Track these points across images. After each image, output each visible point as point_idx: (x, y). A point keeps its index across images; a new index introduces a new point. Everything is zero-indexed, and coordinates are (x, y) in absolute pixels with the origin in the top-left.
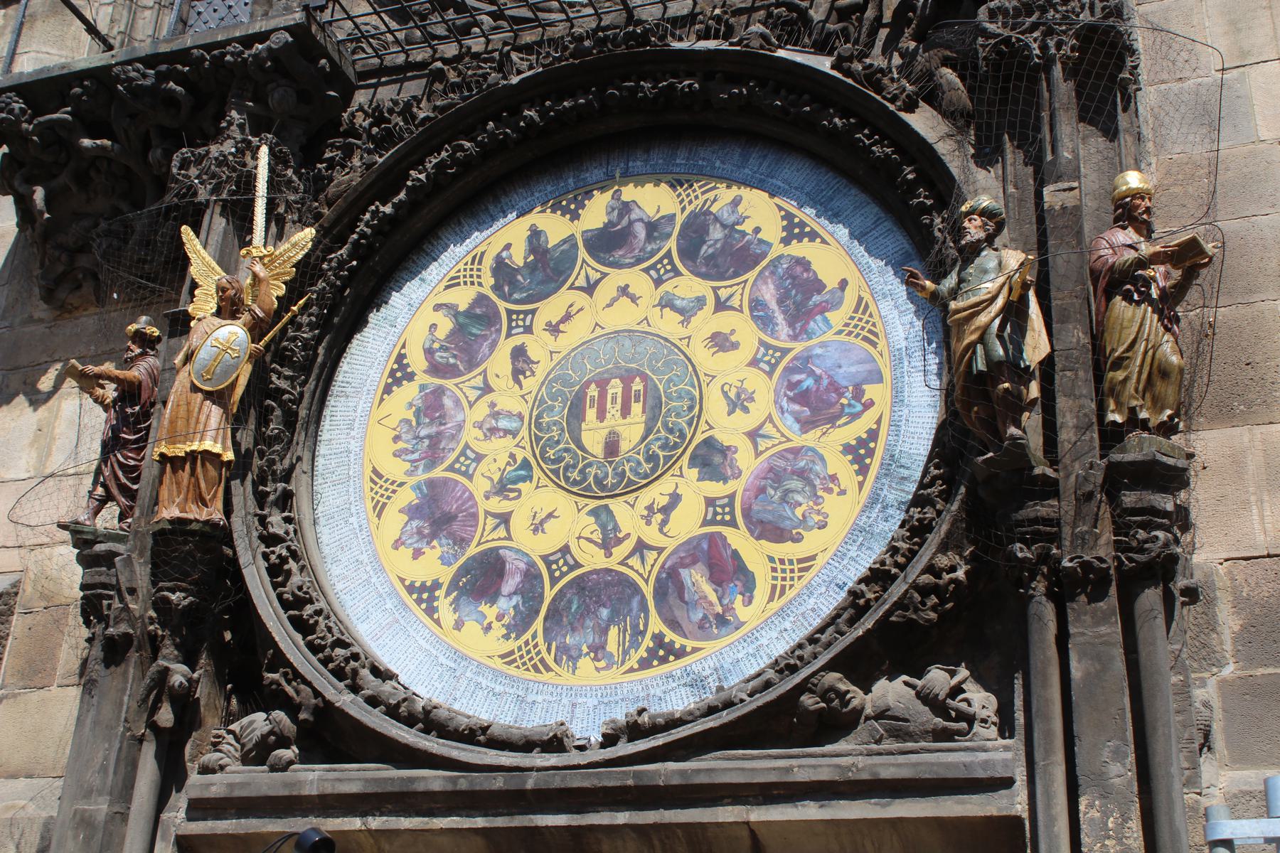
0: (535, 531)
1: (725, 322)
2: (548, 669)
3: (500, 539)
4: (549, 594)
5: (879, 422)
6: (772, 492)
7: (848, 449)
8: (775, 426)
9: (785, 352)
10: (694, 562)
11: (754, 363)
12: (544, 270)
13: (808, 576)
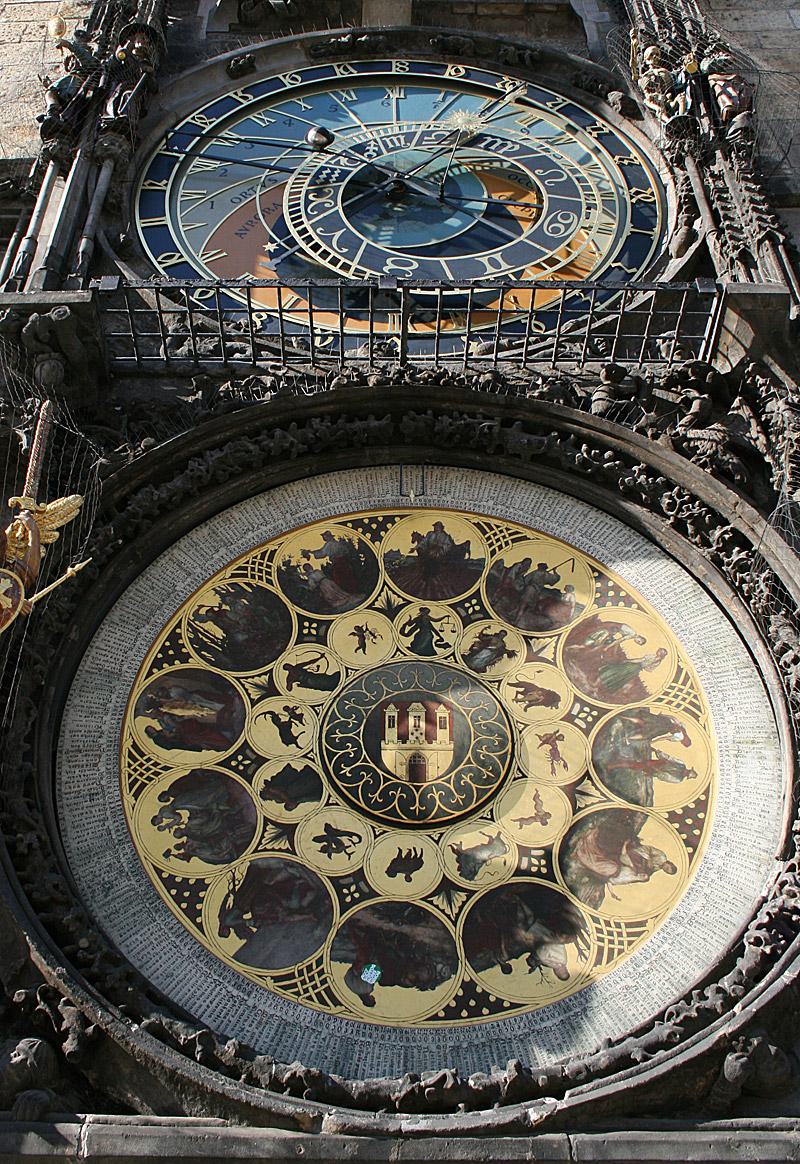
0: (358, 628)
1: (424, 881)
2: (233, 576)
3: (376, 600)
4: (294, 610)
5: (200, 926)
6: (221, 808)
7: (201, 885)
8: (280, 850)
9: (344, 908)
10: (220, 714)
11: (359, 875)
12: (629, 762)
13: (126, 782)
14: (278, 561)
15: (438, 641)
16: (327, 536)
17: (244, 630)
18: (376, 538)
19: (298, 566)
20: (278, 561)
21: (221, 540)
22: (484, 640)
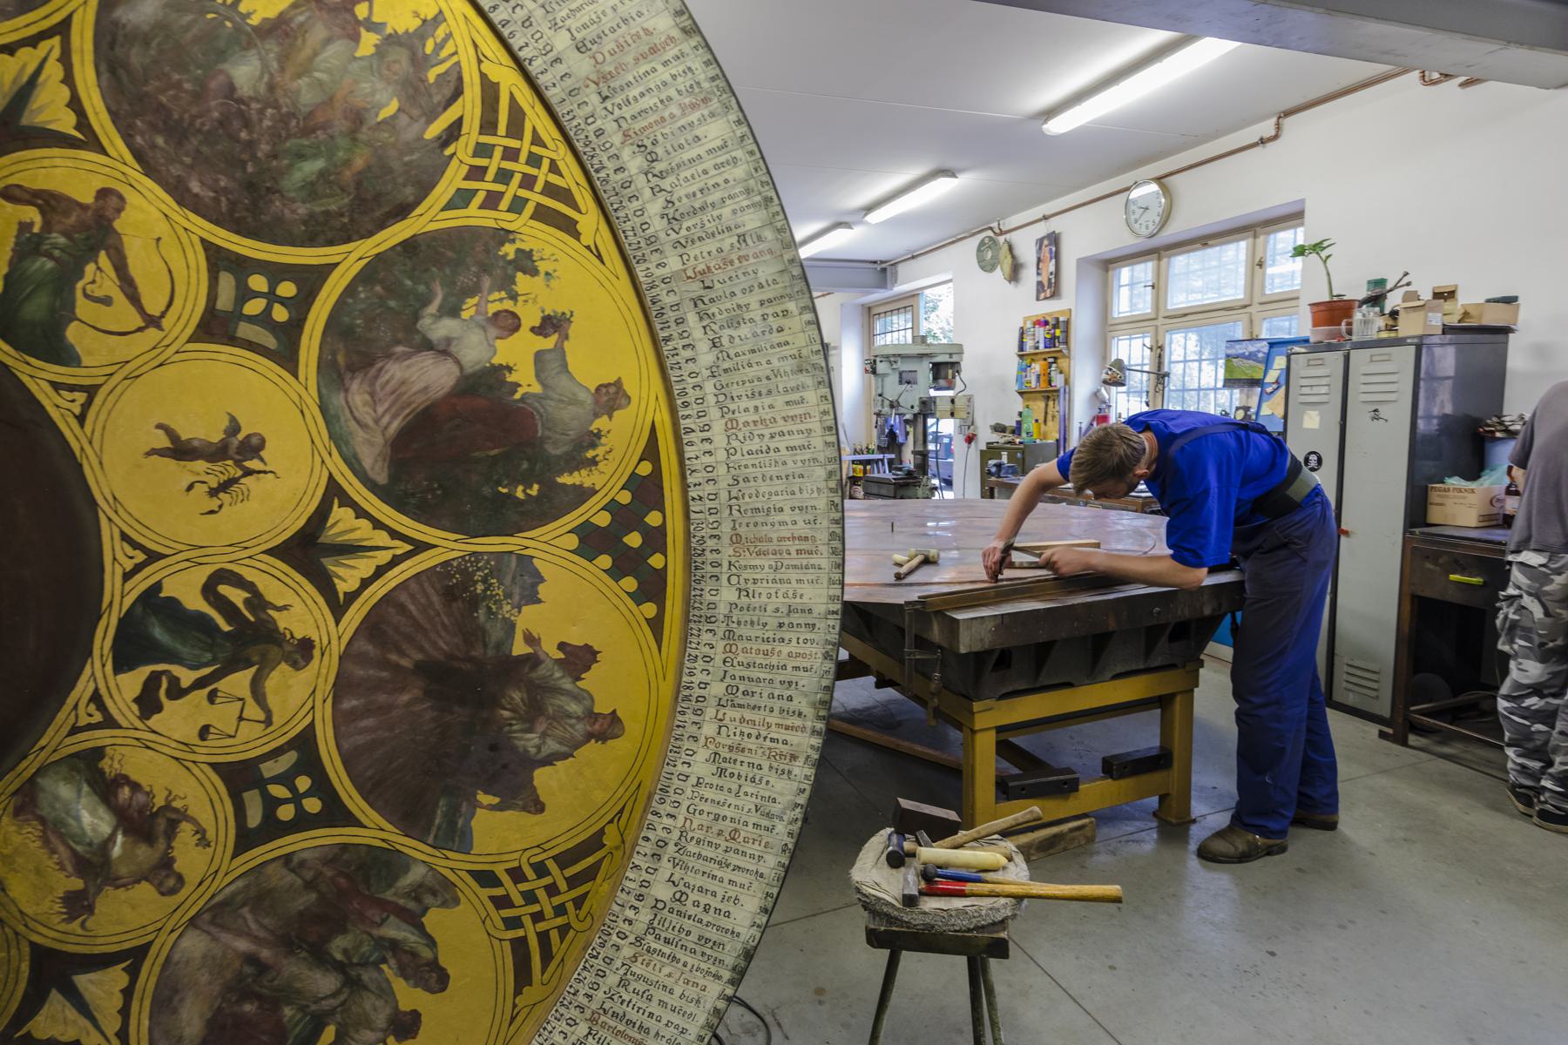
0: (253, 447)
2: (490, 91)
3: (361, 513)
4: (349, 259)
14: (533, 236)
15: (174, 681)
16: (611, 397)
17: (271, 88)
18: (591, 541)
19: (514, 297)
20: (533, 236)
21: (621, 67)
22: (149, 823)
